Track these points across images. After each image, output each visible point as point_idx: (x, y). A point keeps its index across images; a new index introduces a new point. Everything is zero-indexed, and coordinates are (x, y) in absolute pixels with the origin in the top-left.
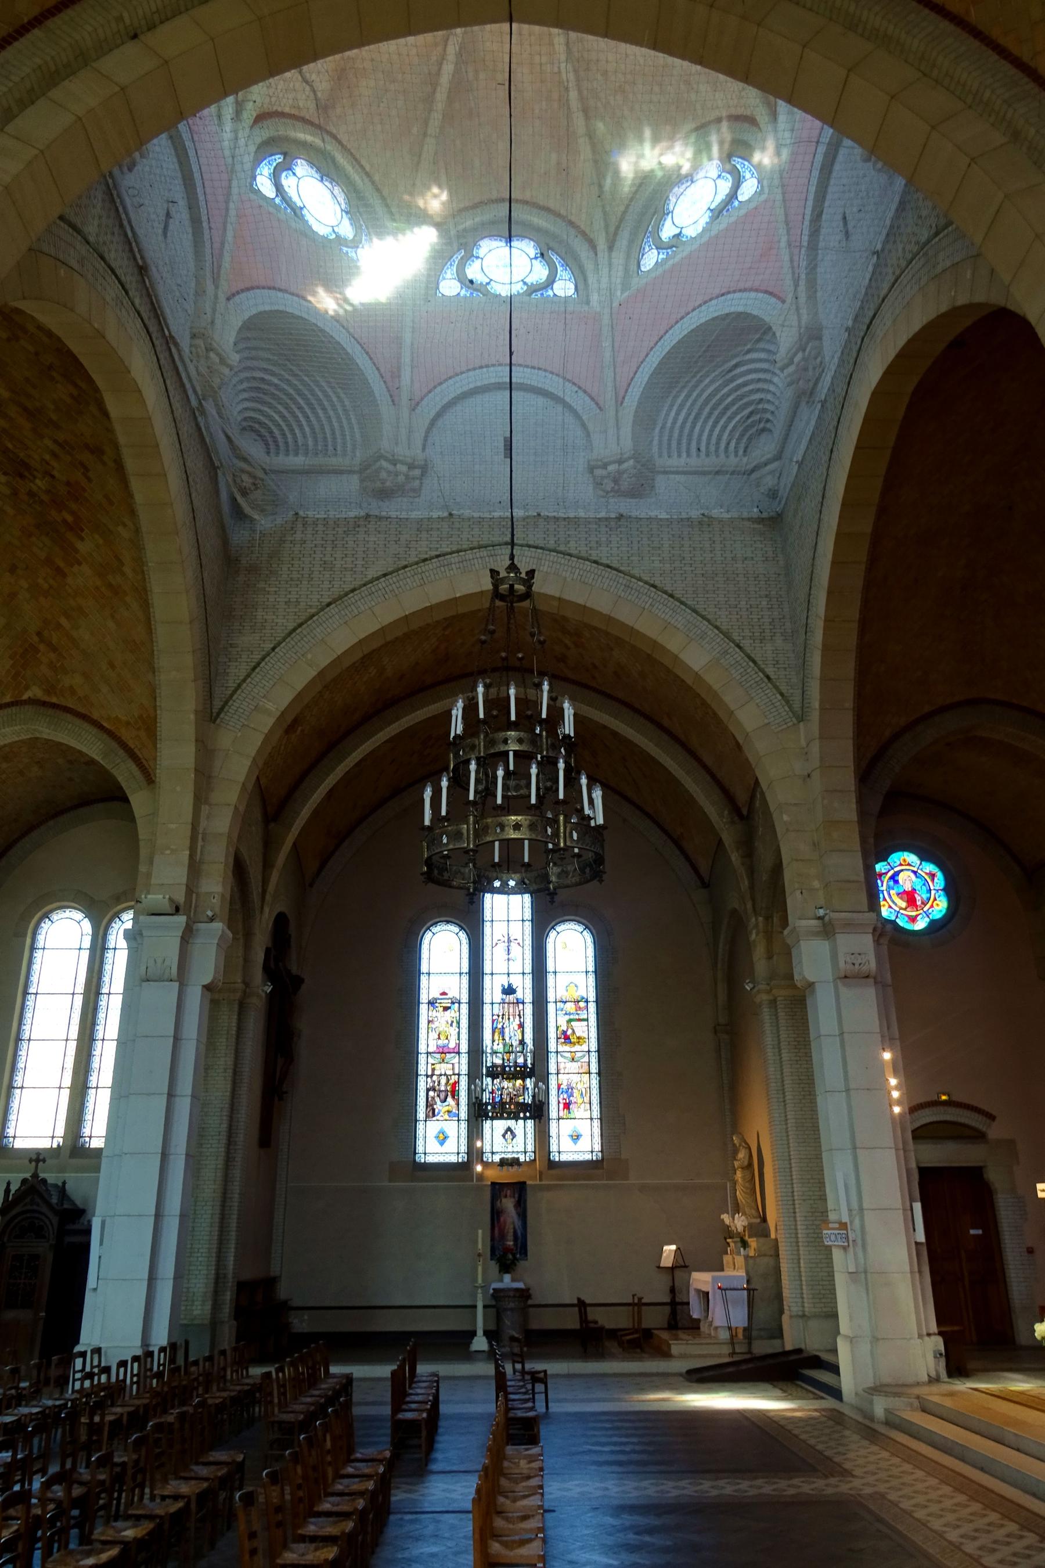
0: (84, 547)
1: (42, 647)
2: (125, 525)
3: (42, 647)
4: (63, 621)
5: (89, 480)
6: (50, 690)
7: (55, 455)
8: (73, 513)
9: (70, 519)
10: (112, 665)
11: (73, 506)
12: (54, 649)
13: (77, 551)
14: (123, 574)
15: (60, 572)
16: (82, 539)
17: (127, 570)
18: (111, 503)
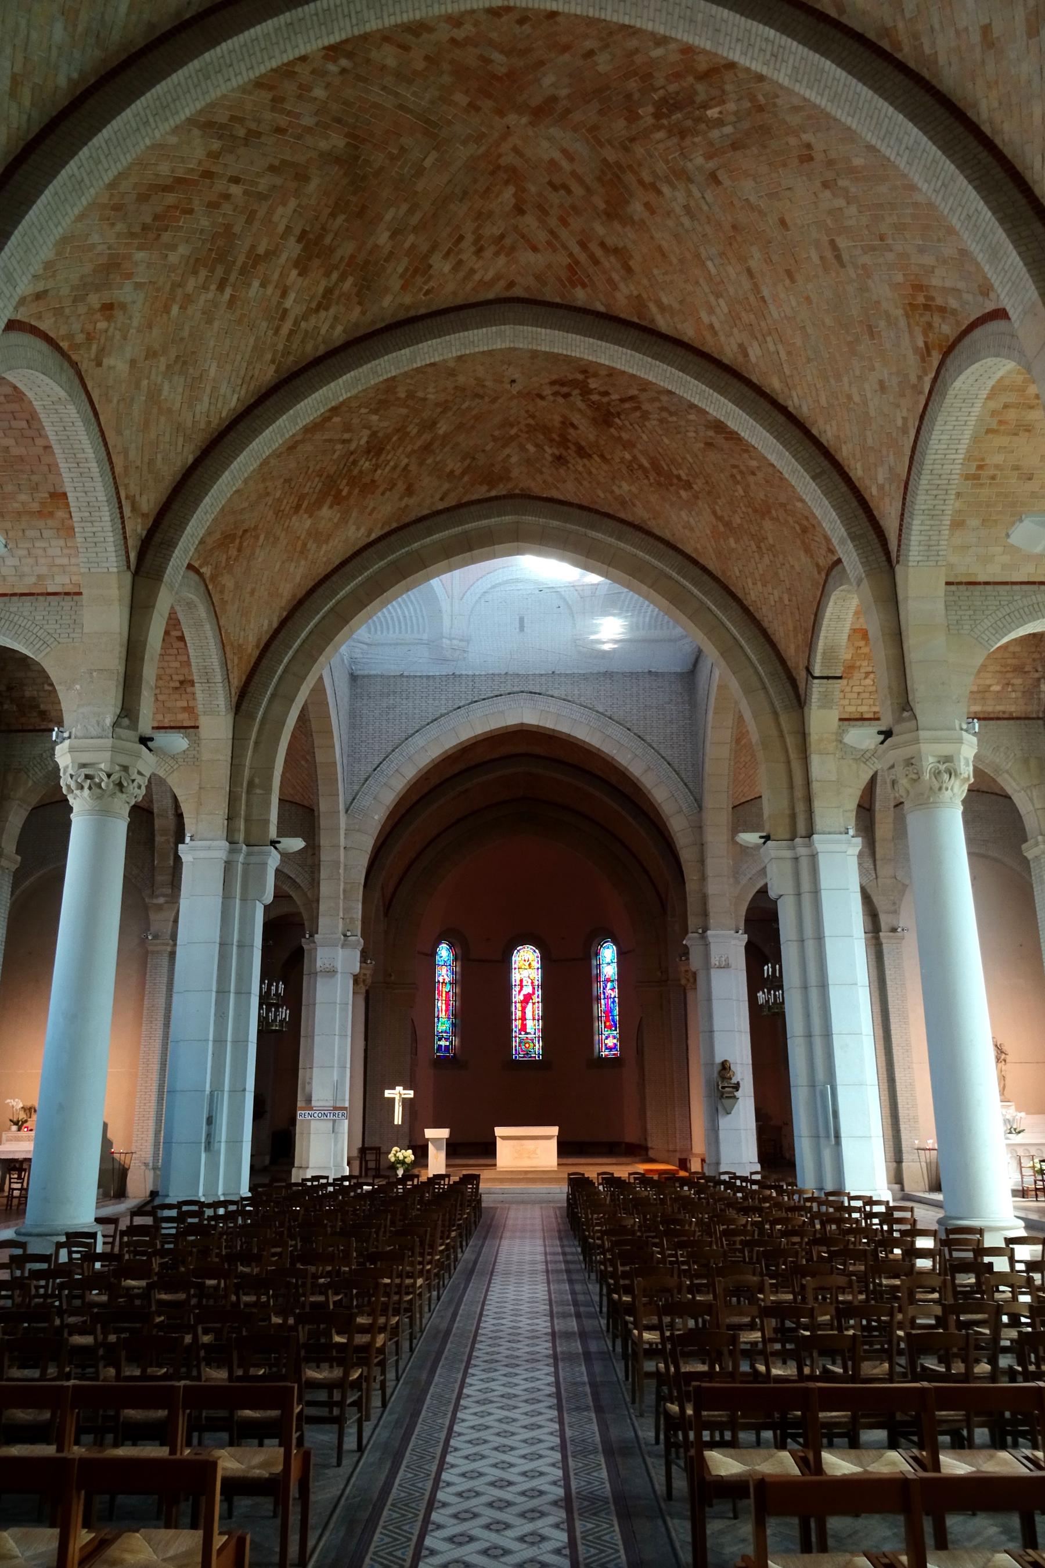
0: (325, 512)
1: (237, 541)
2: (358, 529)
3: (237, 541)
4: (262, 537)
5: (383, 494)
6: (214, 577)
7: (395, 468)
8: (350, 493)
9: (344, 493)
10: (252, 593)
11: (356, 491)
12: (239, 550)
13: (319, 508)
14: (319, 547)
15: (297, 508)
16: (331, 507)
17: (324, 547)
18: (370, 514)
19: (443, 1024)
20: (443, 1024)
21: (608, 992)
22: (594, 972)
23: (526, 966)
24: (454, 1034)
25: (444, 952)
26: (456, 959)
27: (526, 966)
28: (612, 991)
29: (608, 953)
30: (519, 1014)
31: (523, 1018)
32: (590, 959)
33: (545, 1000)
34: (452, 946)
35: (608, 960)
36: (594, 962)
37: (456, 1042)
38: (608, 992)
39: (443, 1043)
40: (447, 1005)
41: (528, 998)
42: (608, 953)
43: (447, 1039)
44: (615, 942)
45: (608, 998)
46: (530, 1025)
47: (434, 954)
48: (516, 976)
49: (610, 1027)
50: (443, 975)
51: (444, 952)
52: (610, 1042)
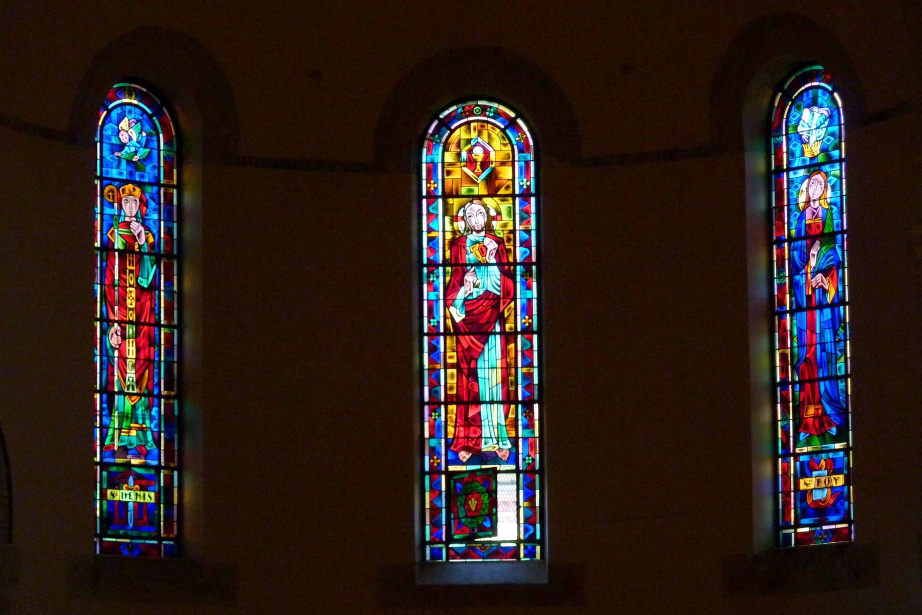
19: (128, 425)
20: (128, 425)
21: (813, 281)
22: (758, 203)
23: (478, 190)
24: (175, 458)
25: (127, 130)
26: (178, 159)
27: (478, 190)
28: (822, 277)
29: (814, 125)
30: (449, 379)
31: (468, 399)
32: (740, 148)
33: (552, 323)
34: (160, 106)
35: (813, 149)
36: (757, 164)
37: (189, 492)
38: (813, 281)
39: (127, 495)
40: (147, 343)
41: (483, 318)
42: (814, 125)
43: (144, 483)
44: (841, 81)
45: (813, 306)
46: (492, 417)
47: (81, 134)
48: (437, 227)
49: (820, 429)
50: (128, 217)
51: (127, 130)
52: (819, 486)
